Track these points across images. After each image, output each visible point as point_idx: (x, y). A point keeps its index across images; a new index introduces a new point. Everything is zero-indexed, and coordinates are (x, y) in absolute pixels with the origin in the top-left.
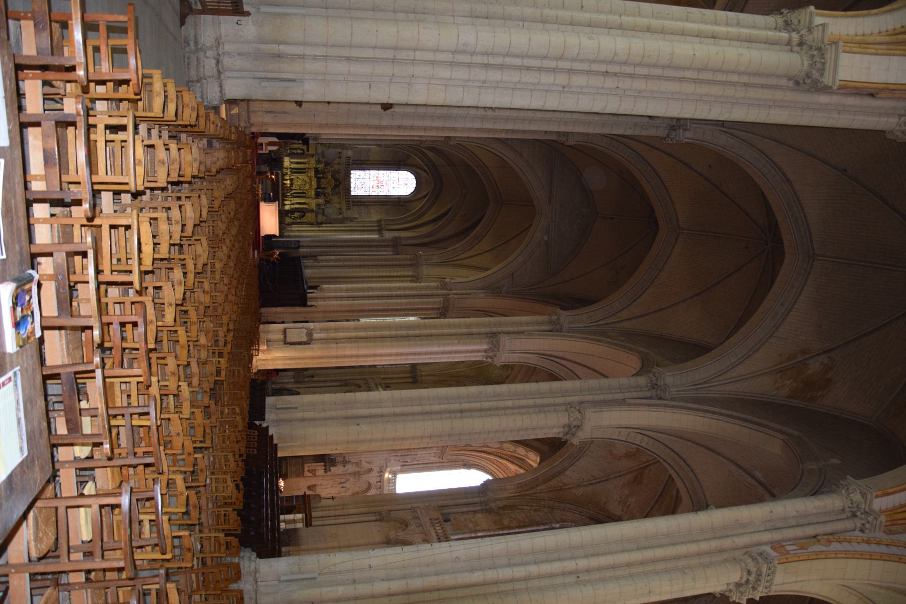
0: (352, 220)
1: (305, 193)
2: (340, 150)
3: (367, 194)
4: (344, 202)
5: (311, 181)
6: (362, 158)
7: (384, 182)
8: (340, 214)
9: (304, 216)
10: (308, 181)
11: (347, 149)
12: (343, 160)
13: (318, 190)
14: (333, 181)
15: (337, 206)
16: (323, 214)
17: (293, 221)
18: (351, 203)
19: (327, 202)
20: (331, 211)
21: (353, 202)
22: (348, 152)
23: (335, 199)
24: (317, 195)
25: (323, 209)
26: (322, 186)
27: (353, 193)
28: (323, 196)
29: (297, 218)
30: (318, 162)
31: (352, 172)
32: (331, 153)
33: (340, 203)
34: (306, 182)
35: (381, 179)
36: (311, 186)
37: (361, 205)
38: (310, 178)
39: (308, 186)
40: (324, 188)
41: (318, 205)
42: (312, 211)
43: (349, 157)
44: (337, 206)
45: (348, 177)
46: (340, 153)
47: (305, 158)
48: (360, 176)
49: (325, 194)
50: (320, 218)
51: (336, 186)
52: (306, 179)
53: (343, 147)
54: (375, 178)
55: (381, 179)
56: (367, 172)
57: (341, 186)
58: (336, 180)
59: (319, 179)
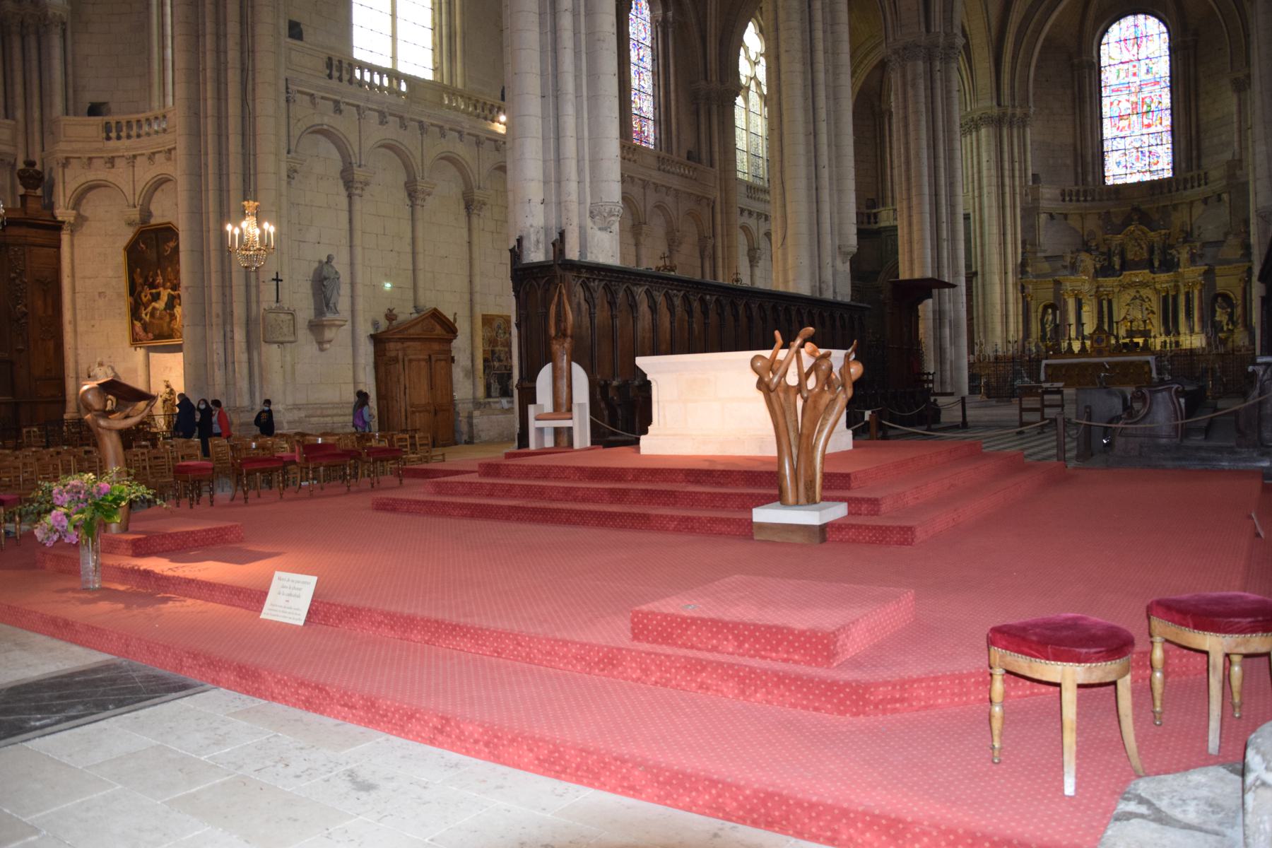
0: (1236, 165)
1: (1165, 299)
2: (1043, 217)
3: (1167, 138)
4: (1188, 192)
5: (1132, 285)
6: (1069, 161)
7: (1133, 99)
8: (1219, 199)
9: (1226, 297)
10: (1132, 292)
11: (1036, 200)
12: (1071, 207)
13: (1156, 264)
14: (1132, 228)
15: (1198, 209)
16: (1218, 244)
17: (1240, 326)
18: (1189, 175)
19: (1188, 237)
20: (1211, 225)
21: (1189, 168)
22: (1048, 196)
23: (1179, 219)
24: (1169, 265)
25: (1205, 244)
26: (1146, 255)
27: (1168, 174)
29: (1231, 316)
30: (1073, 268)
31: (1110, 181)
32: (1049, 239)
33: (1192, 203)
34: (1134, 298)
35: (1125, 107)
36: (1144, 285)
37: (1199, 149)
38: (1124, 287)
39: (1146, 292)
40: (1151, 251)
41: (1193, 260)
42: (1209, 274)
43: (1063, 194)
44: (1198, 209)
45: (1117, 189)
46: (1051, 216)
47: (1065, 303)
48: (1118, 164)
49: (1166, 248)
50: (1232, 250)
51: (1144, 219)
52: (1127, 297)
53: (1030, 212)
54: (1124, 123)
55: (1125, 107)
56: (1107, 146)
57: (1143, 207)
58: (1127, 222)
59: (1125, 266)
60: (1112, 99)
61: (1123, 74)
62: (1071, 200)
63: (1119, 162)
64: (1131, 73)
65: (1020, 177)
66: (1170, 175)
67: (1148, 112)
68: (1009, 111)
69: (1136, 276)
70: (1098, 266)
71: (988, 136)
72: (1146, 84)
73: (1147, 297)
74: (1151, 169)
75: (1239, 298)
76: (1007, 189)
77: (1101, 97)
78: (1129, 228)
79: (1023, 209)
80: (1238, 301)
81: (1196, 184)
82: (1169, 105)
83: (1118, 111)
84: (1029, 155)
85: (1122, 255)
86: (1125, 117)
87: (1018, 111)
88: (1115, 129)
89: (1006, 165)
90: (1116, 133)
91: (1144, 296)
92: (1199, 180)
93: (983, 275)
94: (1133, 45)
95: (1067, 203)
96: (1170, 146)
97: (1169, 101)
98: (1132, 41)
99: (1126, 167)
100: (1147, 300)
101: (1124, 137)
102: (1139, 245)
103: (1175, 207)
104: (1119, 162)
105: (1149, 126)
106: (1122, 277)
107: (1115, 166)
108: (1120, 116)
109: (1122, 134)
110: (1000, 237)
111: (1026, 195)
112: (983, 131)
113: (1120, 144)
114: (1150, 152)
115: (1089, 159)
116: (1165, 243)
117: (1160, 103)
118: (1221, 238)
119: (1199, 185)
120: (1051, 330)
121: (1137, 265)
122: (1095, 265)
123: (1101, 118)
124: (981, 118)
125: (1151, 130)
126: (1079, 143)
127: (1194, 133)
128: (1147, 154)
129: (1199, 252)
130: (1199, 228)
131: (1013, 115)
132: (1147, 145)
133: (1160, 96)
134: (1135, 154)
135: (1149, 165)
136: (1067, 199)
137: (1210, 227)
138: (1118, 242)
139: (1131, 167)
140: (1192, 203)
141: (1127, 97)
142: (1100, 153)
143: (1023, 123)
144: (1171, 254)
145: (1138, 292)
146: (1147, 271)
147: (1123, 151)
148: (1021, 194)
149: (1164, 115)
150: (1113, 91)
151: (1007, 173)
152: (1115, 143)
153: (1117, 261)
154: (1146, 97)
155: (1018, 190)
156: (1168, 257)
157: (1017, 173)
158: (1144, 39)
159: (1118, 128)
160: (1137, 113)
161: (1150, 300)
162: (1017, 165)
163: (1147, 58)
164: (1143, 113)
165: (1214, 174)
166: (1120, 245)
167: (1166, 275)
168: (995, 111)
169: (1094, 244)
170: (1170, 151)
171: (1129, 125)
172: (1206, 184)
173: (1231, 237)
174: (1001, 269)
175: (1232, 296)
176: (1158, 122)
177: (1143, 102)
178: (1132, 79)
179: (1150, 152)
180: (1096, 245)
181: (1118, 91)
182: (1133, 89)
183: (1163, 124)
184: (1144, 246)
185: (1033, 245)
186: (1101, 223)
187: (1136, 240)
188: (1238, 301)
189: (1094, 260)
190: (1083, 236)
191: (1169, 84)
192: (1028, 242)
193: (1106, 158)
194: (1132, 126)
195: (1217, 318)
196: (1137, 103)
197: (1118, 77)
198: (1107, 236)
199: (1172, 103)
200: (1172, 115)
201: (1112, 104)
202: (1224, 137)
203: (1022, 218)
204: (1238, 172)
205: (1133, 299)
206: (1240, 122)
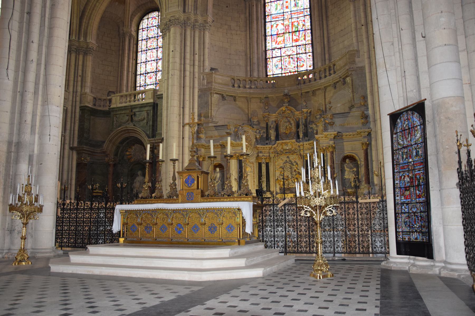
2: (216, 97)
6: (242, 63)
7: (286, 23)
9: (352, 159)
10: (284, 158)
12: (238, 92)
17: (363, 183)
25: (333, 115)
26: (294, 129)
28: (314, 126)
33: (325, 88)
34: (286, 162)
36: (291, 152)
38: (278, 154)
40: (298, 126)
48: (276, 66)
52: (280, 162)
54: (280, 39)
55: (281, 28)
56: (269, 54)
60: (273, 23)
61: (279, 7)
62: (239, 87)
63: (277, 65)
64: (285, 6)
65: (199, 67)
68: (193, 17)
69: (286, 144)
70: (258, 137)
71: (175, 33)
72: (294, 13)
73: (295, 162)
74: (299, 70)
75: (363, 160)
76: (188, 73)
77: (265, 22)
78: (281, 108)
79: (200, 90)
80: (362, 162)
81: (327, 74)
82: (309, 27)
83: (276, 31)
84: (207, 51)
85: (277, 129)
86: (281, 35)
87: (200, 19)
88: (274, 43)
89: (188, 56)
90: (274, 45)
91: (293, 161)
92: (330, 70)
93: (166, 139)
95: (236, 88)
96: (311, 54)
97: (309, 24)
99: (281, 68)
100: (295, 164)
101: (280, 48)
102: (289, 121)
103: (314, 92)
104: (277, 65)
105: (296, 41)
106: (276, 145)
107: (274, 68)
109: (279, 46)
110: (180, 110)
111: (203, 79)
112: (172, 29)
113: (277, 53)
115: (255, 60)
116: (306, 120)
117: (303, 25)
118: (347, 111)
119: (330, 74)
120: (218, 185)
121: (287, 136)
122: (256, 136)
123: (265, 36)
124: (170, 21)
125: (297, 44)
126: (248, 50)
127: (326, 43)
128: (296, 59)
129: (330, 121)
130: (330, 103)
131: (196, 21)
132: (295, 53)
133: (304, 21)
134: (287, 59)
135: (297, 67)
136: (236, 85)
137: (339, 105)
138: (274, 119)
139: (285, 69)
140: (325, 88)
141: (282, 22)
142: (264, 59)
143: (203, 28)
144: (312, 128)
145: (288, 157)
146: (294, 140)
147: (280, 58)
148: (199, 78)
149: (306, 33)
150: (273, 18)
151: (188, 61)
152: (274, 52)
153: (272, 133)
154: (294, 22)
155: (197, 75)
156: (310, 131)
157: (197, 63)
159: (276, 42)
160: (289, 32)
161: (297, 164)
162: (197, 57)
165: (340, 63)
166: (275, 122)
167: (307, 143)
168: (182, 17)
169: (255, 120)
170: (311, 57)
171: (284, 40)
172: (335, 72)
173: (354, 110)
174: (179, 135)
175: (357, 158)
176: (302, 38)
177: (292, 25)
178: (286, 10)
179: (297, 58)
180: (258, 121)
181: (276, 18)
182: (286, 17)
183: (306, 40)
184: (292, 122)
185: (207, 117)
186: (262, 105)
187: (287, 117)
188: (362, 162)
189: (256, 132)
190: (248, 114)
191: (309, 13)
192: (203, 115)
193: (269, 63)
194: (286, 41)
195: (346, 176)
196: (288, 26)
197: (276, 9)
198: (265, 114)
199: (311, 25)
200: (312, 33)
201: (272, 26)
202: (346, 43)
203: (199, 97)
204: (357, 60)
205: (285, 163)
206: (356, 23)
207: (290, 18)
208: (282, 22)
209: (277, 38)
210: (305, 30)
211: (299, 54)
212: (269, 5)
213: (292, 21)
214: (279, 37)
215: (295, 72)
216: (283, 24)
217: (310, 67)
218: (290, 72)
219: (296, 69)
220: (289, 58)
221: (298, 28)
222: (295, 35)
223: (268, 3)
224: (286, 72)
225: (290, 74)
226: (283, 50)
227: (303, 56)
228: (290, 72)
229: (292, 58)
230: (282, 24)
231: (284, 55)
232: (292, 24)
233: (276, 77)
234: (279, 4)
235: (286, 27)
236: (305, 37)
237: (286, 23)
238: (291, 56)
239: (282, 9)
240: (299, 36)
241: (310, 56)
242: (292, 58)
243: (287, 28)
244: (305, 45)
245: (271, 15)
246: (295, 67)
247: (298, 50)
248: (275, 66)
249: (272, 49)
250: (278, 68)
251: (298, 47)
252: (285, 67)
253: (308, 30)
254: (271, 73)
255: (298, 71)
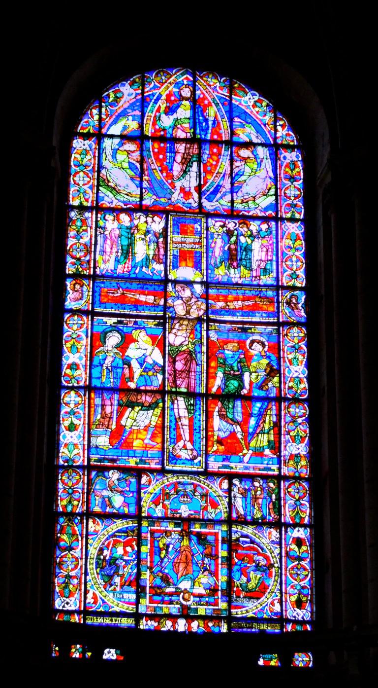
7: (178, 337)
63: (113, 562)
66: (296, 655)
67: (225, 397)
74: (237, 613)
86: (147, 399)
94: (187, 162)
98: (181, 148)
107: (95, 579)
108: (122, 390)
114: (232, 545)
117: (273, 371)
139: (156, 590)
147: (131, 524)
158: (225, 153)
163: (231, 214)
164: (207, 395)
179: (232, 545)
196: (190, 356)
200: (312, 420)
201: (97, 340)
207: (199, 320)
208: (159, 331)
209: (123, 407)
210: (279, 399)
211: (243, 521)
212: (84, 222)
213: (213, 336)
214: (132, 405)
215: (216, 618)
216: (161, 343)
217: (299, 604)
218: (187, 614)
219: (223, 605)
220: (186, 534)
221: (240, 378)
222: (222, 417)
223: (82, 208)
224: (165, 609)
225: (181, 625)
226: (153, 486)
227: (267, 538)
228: (187, 614)
229: (201, 538)
230: (153, 338)
231: (159, 512)
232: (213, 351)
233: (100, 626)
234: (143, 227)
235: (174, 362)
236: (278, 434)
237: (178, 337)
238: (197, 528)
239: (156, 258)
240: (244, 424)
241: (299, 542)
242: (201, 538)
243: (179, 365)
244: (279, 478)
245: (94, 277)
246: (213, 591)
247: (239, 502)
248: (101, 563)
249: (89, 468)
250: (117, 580)
251: (236, 481)
252: (158, 581)
253: (295, 400)
254: (73, 604)
255: (230, 619)
